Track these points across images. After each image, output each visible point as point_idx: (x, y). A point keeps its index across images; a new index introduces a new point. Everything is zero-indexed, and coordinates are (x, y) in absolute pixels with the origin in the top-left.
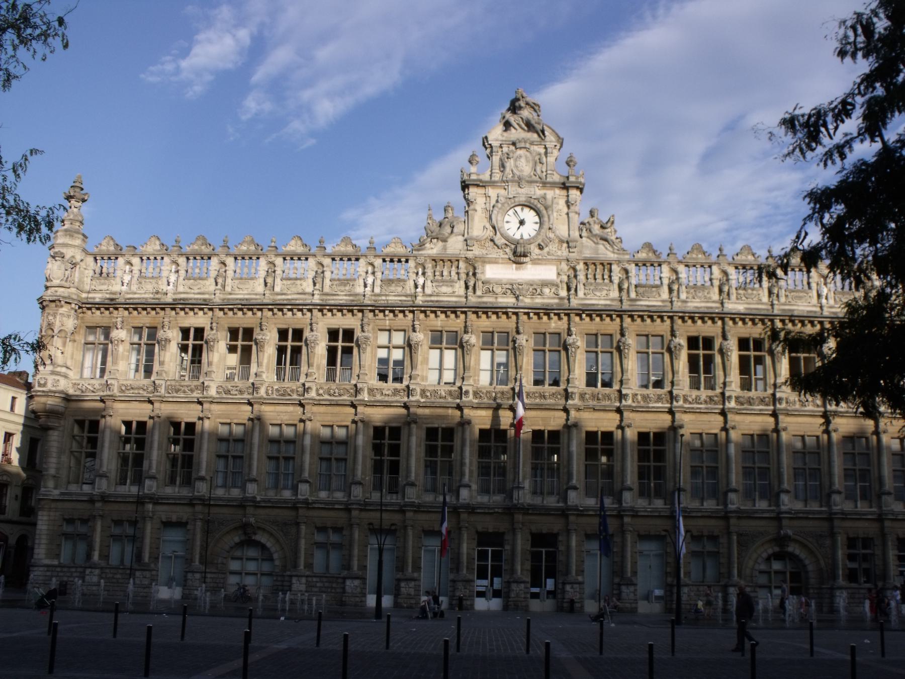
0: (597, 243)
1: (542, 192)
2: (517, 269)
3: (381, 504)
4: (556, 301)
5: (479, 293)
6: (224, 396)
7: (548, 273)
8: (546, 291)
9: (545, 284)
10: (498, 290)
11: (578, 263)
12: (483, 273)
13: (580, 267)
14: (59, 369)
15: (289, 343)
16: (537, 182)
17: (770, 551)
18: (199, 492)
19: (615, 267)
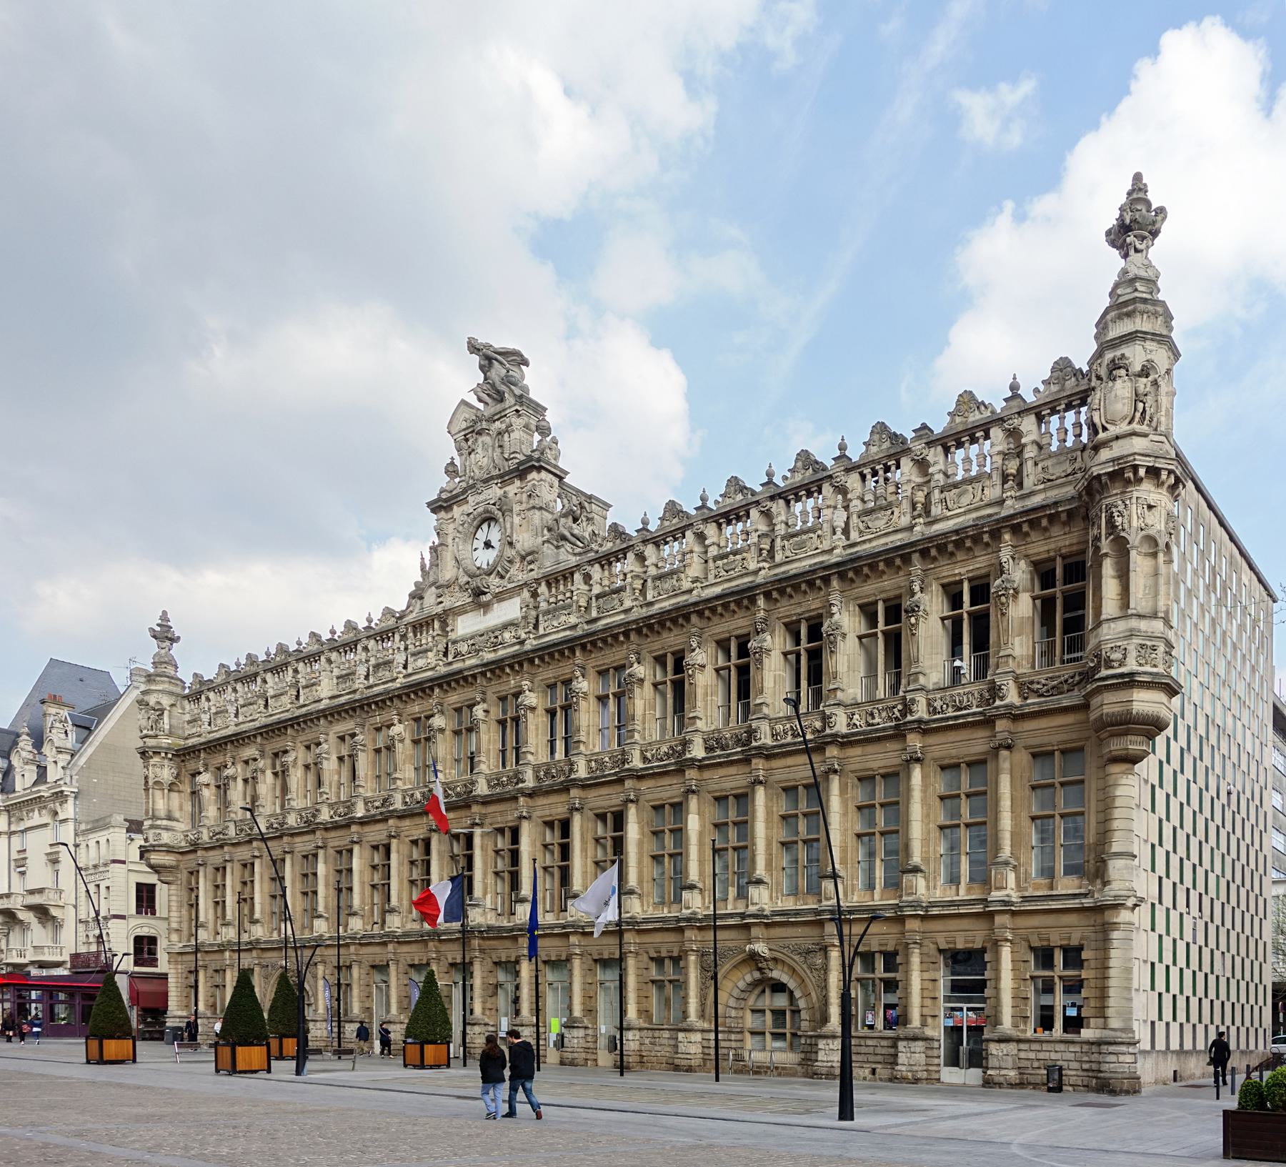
0: (558, 547)
1: (500, 492)
2: (485, 613)
3: (715, 917)
4: (517, 647)
5: (450, 659)
6: (718, 752)
7: (510, 610)
8: (507, 635)
9: (505, 627)
10: (463, 648)
11: (540, 584)
12: (452, 630)
13: (543, 589)
14: (159, 822)
15: (1058, 590)
16: (492, 478)
17: (749, 978)
18: (688, 908)
19: (577, 577)
